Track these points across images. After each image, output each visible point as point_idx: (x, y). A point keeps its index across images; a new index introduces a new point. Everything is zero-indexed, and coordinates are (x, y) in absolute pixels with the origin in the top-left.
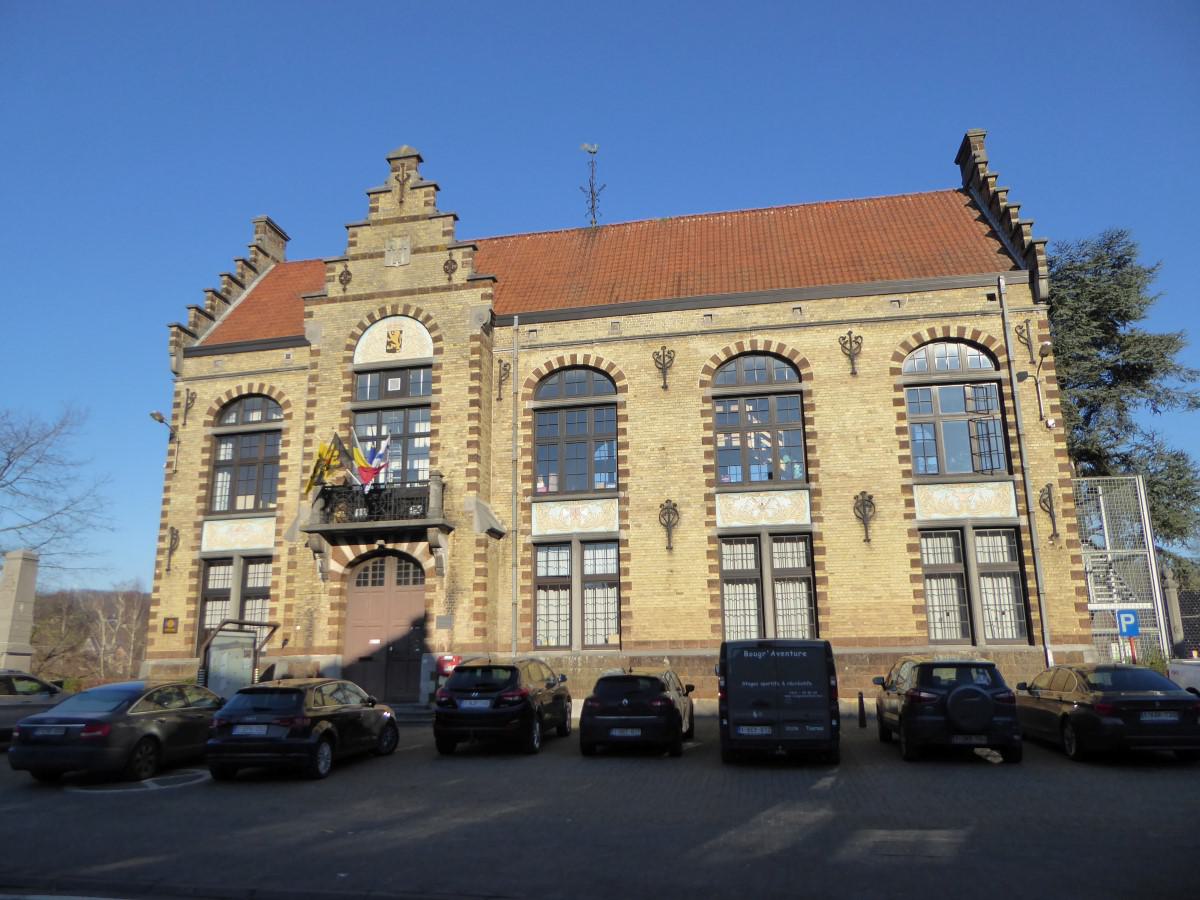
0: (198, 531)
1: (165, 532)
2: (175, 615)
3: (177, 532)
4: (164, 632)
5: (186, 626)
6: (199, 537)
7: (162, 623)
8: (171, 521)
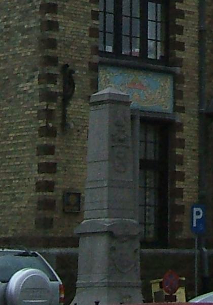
1: (54, 70)
3: (72, 72)
8: (64, 55)
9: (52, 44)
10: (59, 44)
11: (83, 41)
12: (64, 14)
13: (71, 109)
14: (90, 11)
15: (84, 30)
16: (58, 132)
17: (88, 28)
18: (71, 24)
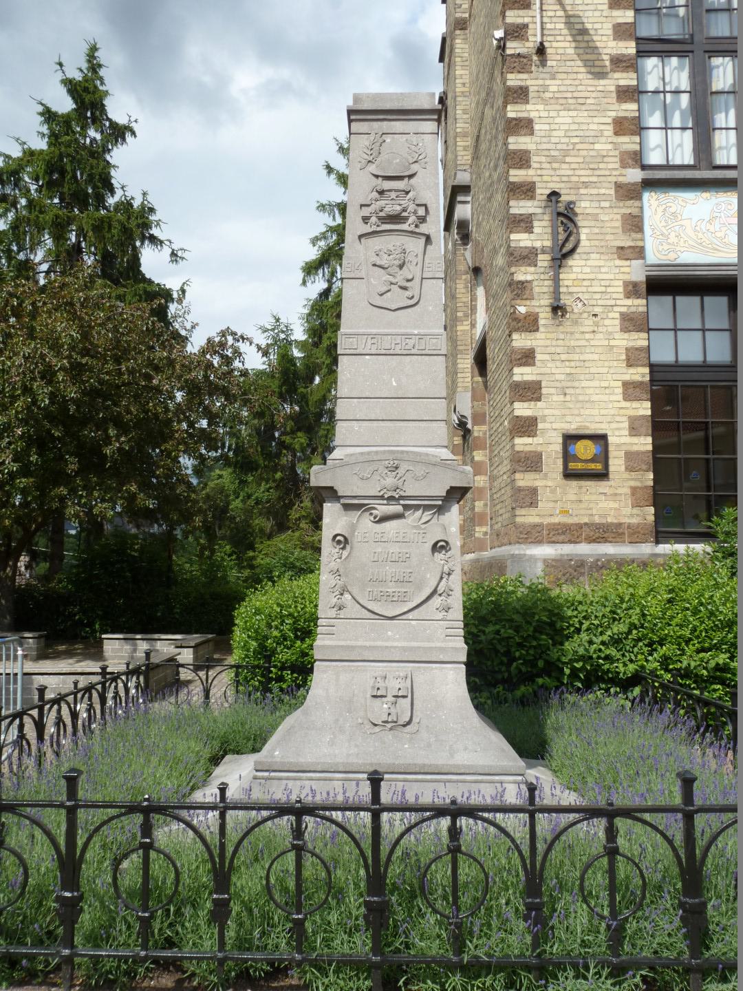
0: (629, 207)
2: (594, 428)
4: (569, 475)
5: (630, 456)
6: (635, 224)
7: (558, 447)
9: (522, 159)
10: (534, 159)
11: (597, 146)
12: (545, 102)
13: (573, 276)
14: (613, 88)
15: (602, 124)
16: (541, 322)
17: (610, 120)
18: (564, 119)
